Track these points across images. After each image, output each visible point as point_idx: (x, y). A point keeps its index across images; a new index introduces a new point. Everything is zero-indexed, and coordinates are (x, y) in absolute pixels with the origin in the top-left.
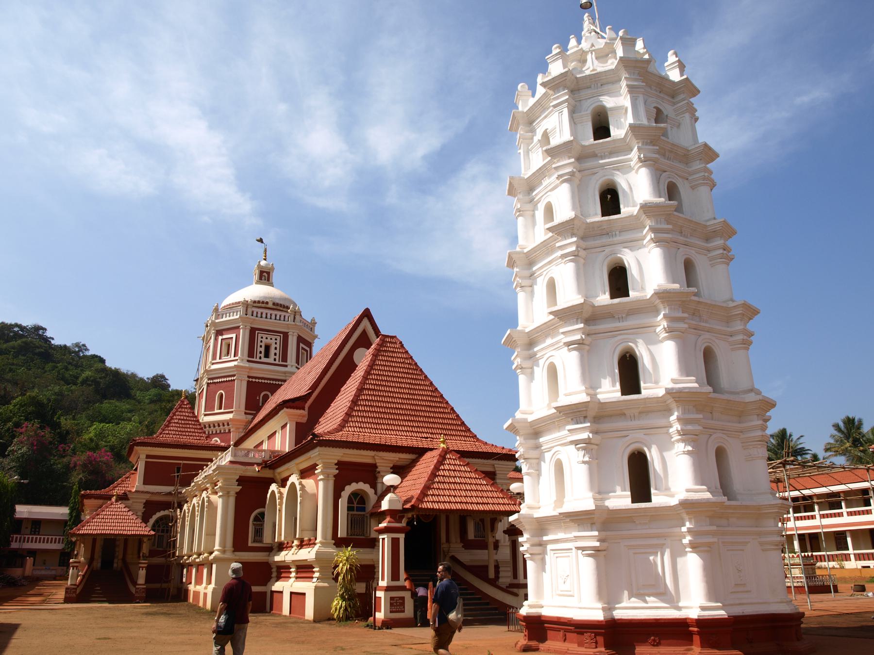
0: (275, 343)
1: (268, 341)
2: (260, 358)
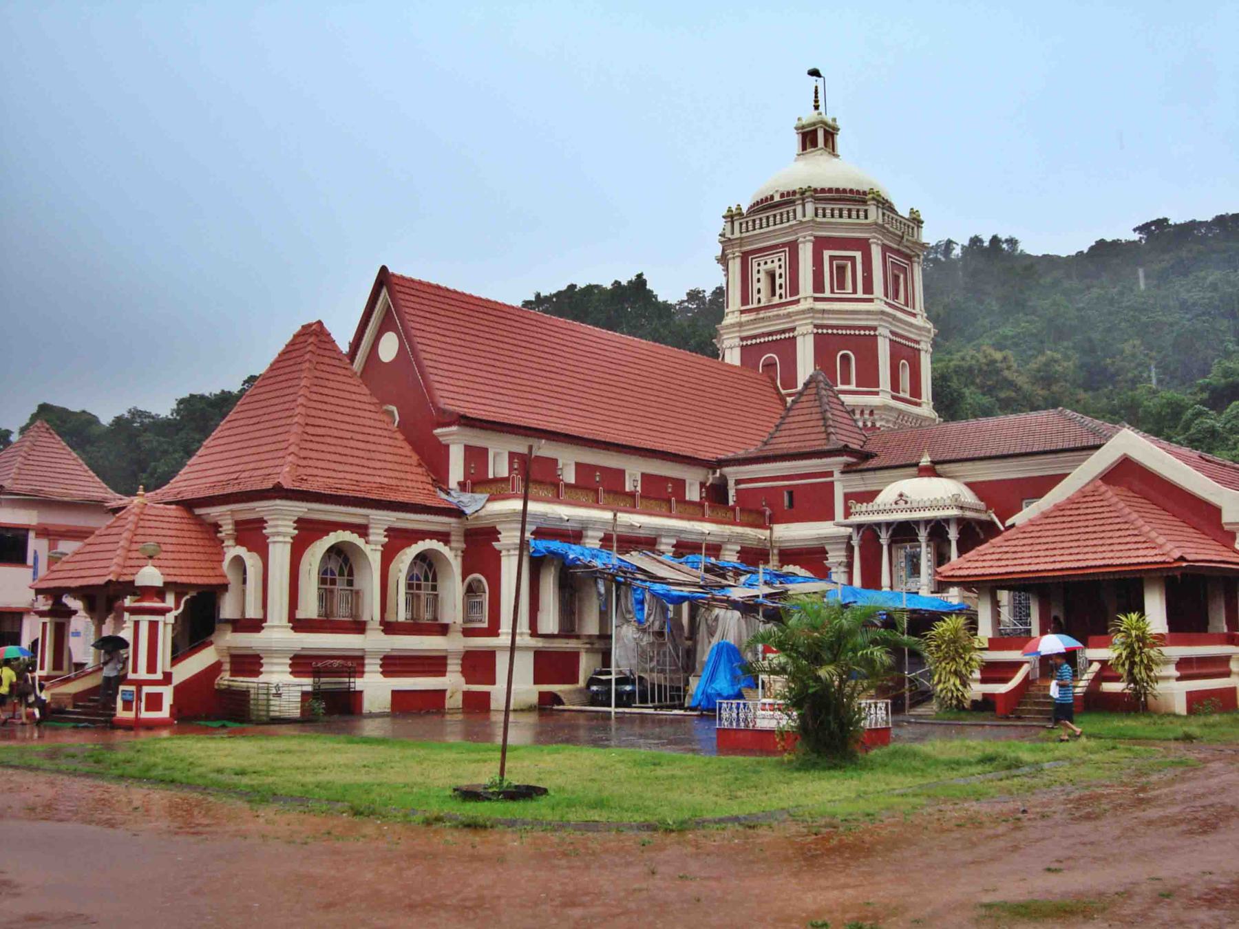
0: (778, 263)
1: (769, 266)
2: (759, 301)
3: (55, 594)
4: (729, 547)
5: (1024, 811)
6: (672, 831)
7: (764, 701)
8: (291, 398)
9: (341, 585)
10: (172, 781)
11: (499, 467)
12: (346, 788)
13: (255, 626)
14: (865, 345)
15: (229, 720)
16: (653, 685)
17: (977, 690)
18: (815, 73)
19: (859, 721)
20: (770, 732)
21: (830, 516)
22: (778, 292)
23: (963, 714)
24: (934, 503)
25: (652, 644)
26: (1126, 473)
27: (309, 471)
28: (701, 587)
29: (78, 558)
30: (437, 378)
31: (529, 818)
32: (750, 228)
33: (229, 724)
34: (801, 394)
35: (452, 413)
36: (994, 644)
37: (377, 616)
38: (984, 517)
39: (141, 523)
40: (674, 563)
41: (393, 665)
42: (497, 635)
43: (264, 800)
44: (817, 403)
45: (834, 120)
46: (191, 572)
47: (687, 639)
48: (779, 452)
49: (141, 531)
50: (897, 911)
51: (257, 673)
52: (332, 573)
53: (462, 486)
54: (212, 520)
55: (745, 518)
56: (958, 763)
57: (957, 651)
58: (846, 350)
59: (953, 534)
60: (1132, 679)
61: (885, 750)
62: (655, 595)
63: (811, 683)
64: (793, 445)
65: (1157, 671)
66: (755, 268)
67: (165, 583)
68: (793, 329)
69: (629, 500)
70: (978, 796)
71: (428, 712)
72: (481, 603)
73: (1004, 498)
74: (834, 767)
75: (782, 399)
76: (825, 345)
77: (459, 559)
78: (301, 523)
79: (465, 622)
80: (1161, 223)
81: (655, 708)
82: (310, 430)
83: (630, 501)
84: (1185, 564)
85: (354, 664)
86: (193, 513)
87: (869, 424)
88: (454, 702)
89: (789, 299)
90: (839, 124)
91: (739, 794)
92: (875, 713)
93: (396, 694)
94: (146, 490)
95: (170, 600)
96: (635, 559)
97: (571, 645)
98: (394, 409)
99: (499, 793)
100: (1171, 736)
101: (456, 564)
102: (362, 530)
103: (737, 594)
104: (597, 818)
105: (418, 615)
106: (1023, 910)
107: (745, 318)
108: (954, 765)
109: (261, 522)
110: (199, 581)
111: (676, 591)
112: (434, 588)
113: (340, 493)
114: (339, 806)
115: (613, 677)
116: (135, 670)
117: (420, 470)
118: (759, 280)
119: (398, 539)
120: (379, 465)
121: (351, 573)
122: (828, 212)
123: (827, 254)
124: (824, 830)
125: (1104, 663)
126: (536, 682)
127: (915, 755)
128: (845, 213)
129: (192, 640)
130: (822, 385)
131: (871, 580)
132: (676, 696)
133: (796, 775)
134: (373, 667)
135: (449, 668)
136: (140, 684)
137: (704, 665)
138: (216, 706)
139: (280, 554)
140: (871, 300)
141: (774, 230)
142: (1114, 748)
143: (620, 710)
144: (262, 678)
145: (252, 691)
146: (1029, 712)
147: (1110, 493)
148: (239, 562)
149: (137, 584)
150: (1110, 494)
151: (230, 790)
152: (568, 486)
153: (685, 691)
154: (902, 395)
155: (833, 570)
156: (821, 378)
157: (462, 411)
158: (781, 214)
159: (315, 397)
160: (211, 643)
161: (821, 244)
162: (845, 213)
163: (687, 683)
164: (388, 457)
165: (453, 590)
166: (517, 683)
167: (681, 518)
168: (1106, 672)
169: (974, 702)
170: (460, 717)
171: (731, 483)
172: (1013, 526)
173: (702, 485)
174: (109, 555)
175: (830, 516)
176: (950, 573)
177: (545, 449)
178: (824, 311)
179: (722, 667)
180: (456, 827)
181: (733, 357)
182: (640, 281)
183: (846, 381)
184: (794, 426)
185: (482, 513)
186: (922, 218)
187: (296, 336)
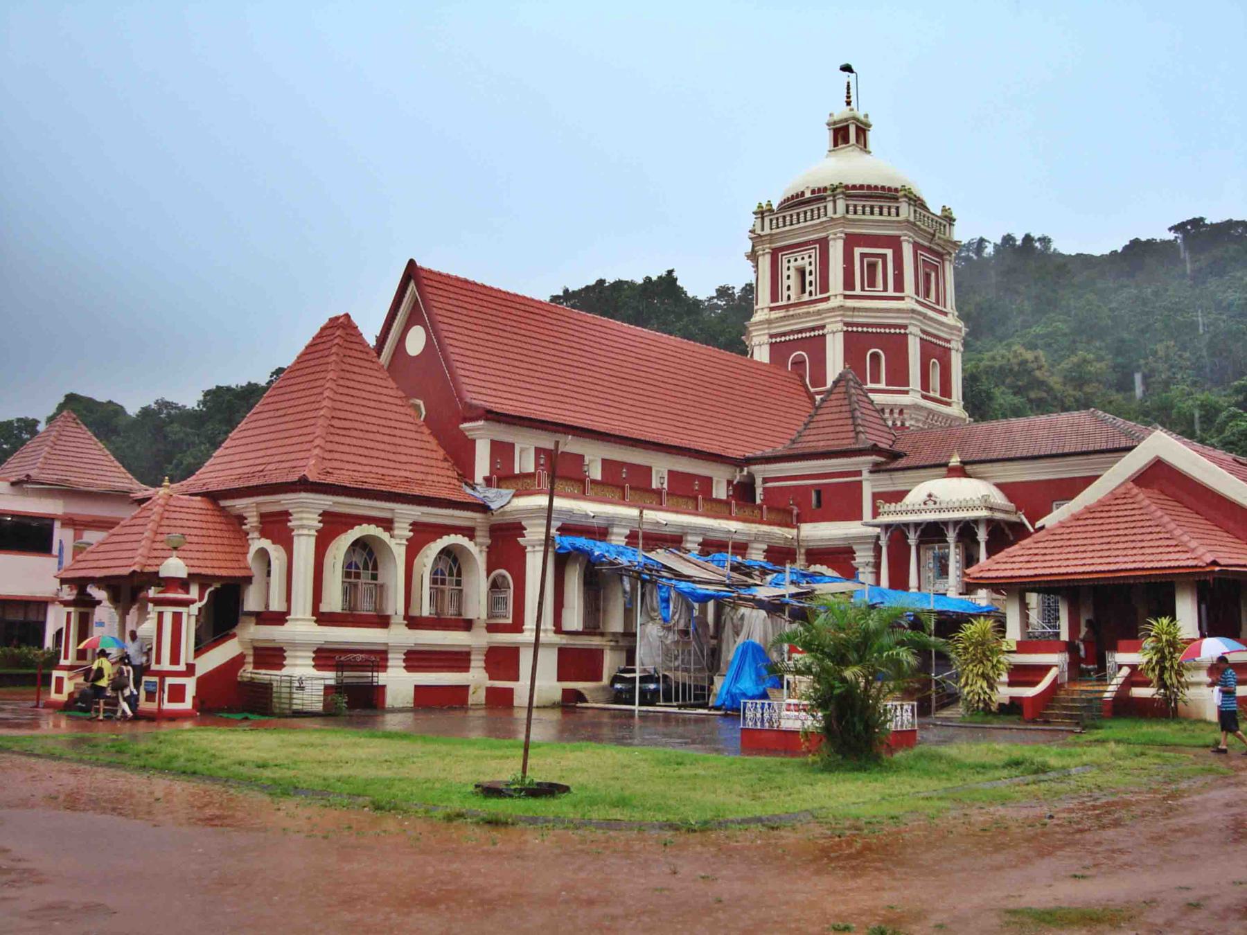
0: (809, 260)
1: (800, 262)
2: (789, 297)
3: (80, 584)
4: (755, 545)
5: (1051, 817)
6: (695, 831)
7: (789, 701)
8: (319, 390)
9: (365, 579)
10: (194, 773)
11: (525, 462)
12: (369, 782)
13: (279, 618)
14: (895, 344)
15: (252, 712)
16: (677, 683)
17: (1004, 693)
18: (847, 69)
19: (885, 722)
20: (795, 733)
21: (859, 517)
22: (808, 289)
23: (989, 718)
24: (963, 504)
25: (677, 643)
26: (1158, 476)
27: (336, 464)
28: (728, 586)
29: (102, 548)
30: (463, 372)
31: (551, 817)
32: (781, 224)
33: (251, 717)
34: (830, 392)
35: (477, 407)
36: (1023, 647)
37: (401, 611)
38: (1013, 518)
39: (166, 515)
40: (700, 561)
41: (417, 659)
42: (520, 630)
43: (285, 793)
44: (846, 402)
45: (866, 116)
46: (215, 564)
47: (712, 638)
48: (807, 451)
49: (165, 522)
50: (919, 916)
51: (280, 666)
52: (357, 567)
53: (488, 481)
54: (237, 512)
55: (773, 516)
56: (984, 767)
57: (984, 654)
58: (876, 348)
59: (982, 535)
60: (1163, 684)
61: (911, 752)
62: (681, 593)
63: (837, 684)
64: (822, 443)
65: (1188, 677)
66: (785, 265)
67: (189, 575)
68: (823, 327)
69: (654, 496)
70: (1004, 800)
71: (451, 708)
72: (505, 600)
73: (1033, 499)
74: (860, 769)
75: (811, 397)
76: (855, 343)
77: (484, 554)
78: (326, 516)
79: (490, 616)
80: (1197, 222)
81: (680, 707)
82: (336, 423)
83: (657, 499)
84: (1217, 569)
85: (378, 659)
86: (218, 505)
87: (899, 424)
88: (477, 697)
89: (819, 296)
90: (871, 120)
91: (762, 794)
92: (900, 715)
93: (419, 689)
94: (171, 481)
95: (194, 592)
96: (660, 556)
97: (595, 642)
98: (421, 403)
99: (521, 790)
100: (1201, 742)
101: (481, 560)
102: (387, 524)
103: (763, 593)
104: (619, 817)
105: (442, 610)
106: (1048, 918)
107: (775, 315)
108: (982, 768)
109: (286, 515)
110: (224, 573)
111: (701, 589)
112: (459, 583)
113: (366, 486)
114: (361, 800)
115: (637, 675)
116: (158, 661)
117: (446, 465)
118: (788, 277)
119: (423, 533)
120: (404, 459)
121: (375, 567)
122: (859, 208)
123: (858, 251)
124: (848, 833)
125: (1133, 667)
126: (560, 679)
127: (940, 758)
128: (876, 210)
129: (216, 632)
130: (852, 383)
131: (899, 581)
132: (700, 696)
133: (820, 776)
134: (396, 662)
135: (473, 664)
136: (163, 675)
137: (729, 664)
138: (239, 698)
139: (304, 547)
140: (902, 298)
141: (804, 227)
142: (1143, 754)
143: (644, 708)
144: (285, 671)
145: (275, 684)
146: (1058, 716)
147: (1142, 496)
148: (263, 554)
149: (161, 575)
150: (1141, 496)
151: (250, 782)
152: (594, 482)
153: (710, 690)
154: (932, 394)
155: (861, 570)
156: (851, 376)
157: (488, 406)
158: (812, 211)
159: (341, 390)
160: (234, 636)
161: (851, 242)
162: (876, 210)
163: (712, 682)
164: (415, 452)
165: (477, 585)
166: (541, 680)
167: (708, 516)
168: (1136, 677)
169: (1001, 705)
170: (482, 713)
171: (759, 481)
172: (1042, 528)
173: (729, 483)
174: (135, 545)
175: (859, 517)
176: (979, 575)
177: (571, 445)
178: (854, 309)
179: (747, 668)
180: (477, 823)
181: (762, 355)
182: (669, 280)
183: (876, 379)
184: (821, 425)
185: (508, 508)
186: (954, 215)
187: (323, 329)
